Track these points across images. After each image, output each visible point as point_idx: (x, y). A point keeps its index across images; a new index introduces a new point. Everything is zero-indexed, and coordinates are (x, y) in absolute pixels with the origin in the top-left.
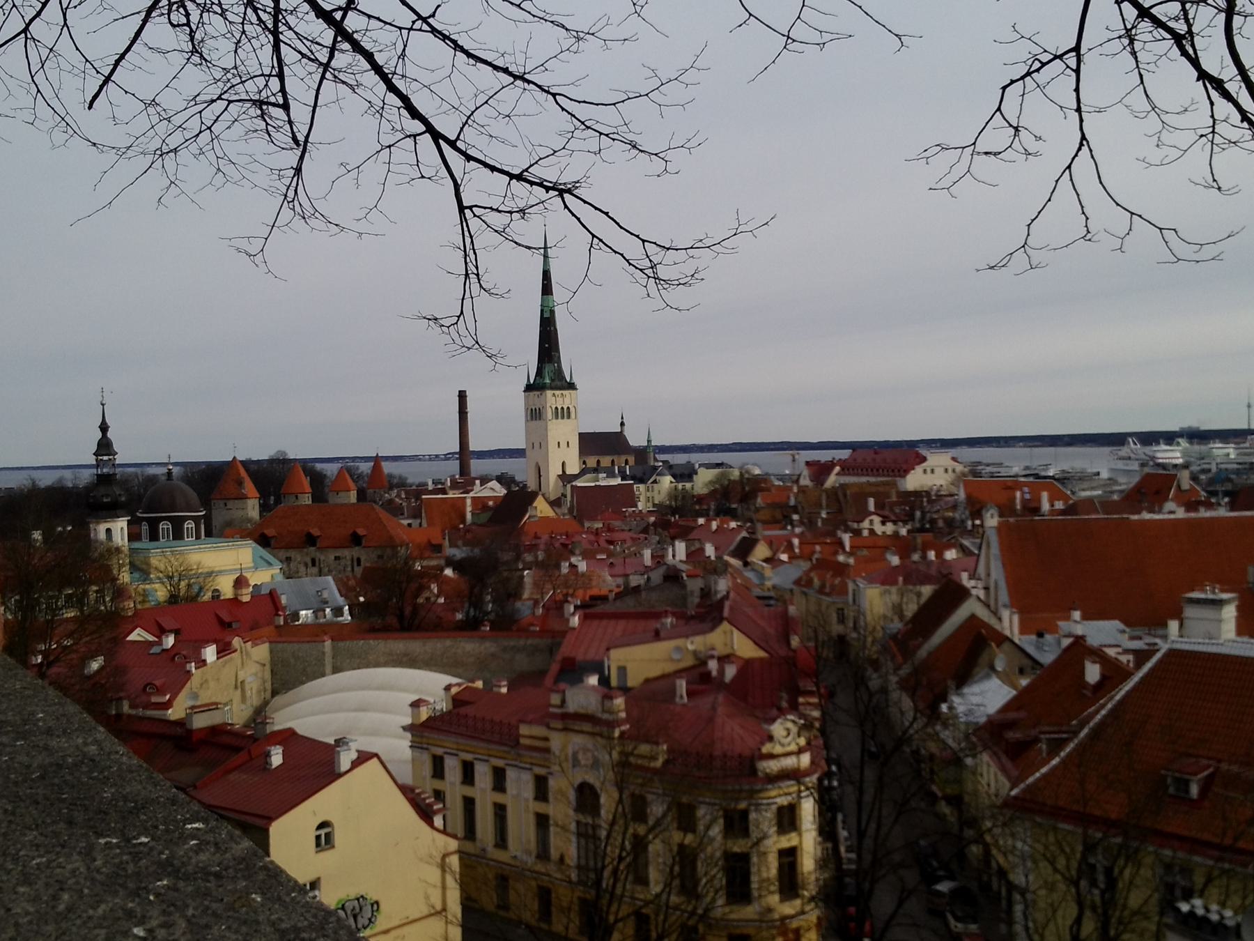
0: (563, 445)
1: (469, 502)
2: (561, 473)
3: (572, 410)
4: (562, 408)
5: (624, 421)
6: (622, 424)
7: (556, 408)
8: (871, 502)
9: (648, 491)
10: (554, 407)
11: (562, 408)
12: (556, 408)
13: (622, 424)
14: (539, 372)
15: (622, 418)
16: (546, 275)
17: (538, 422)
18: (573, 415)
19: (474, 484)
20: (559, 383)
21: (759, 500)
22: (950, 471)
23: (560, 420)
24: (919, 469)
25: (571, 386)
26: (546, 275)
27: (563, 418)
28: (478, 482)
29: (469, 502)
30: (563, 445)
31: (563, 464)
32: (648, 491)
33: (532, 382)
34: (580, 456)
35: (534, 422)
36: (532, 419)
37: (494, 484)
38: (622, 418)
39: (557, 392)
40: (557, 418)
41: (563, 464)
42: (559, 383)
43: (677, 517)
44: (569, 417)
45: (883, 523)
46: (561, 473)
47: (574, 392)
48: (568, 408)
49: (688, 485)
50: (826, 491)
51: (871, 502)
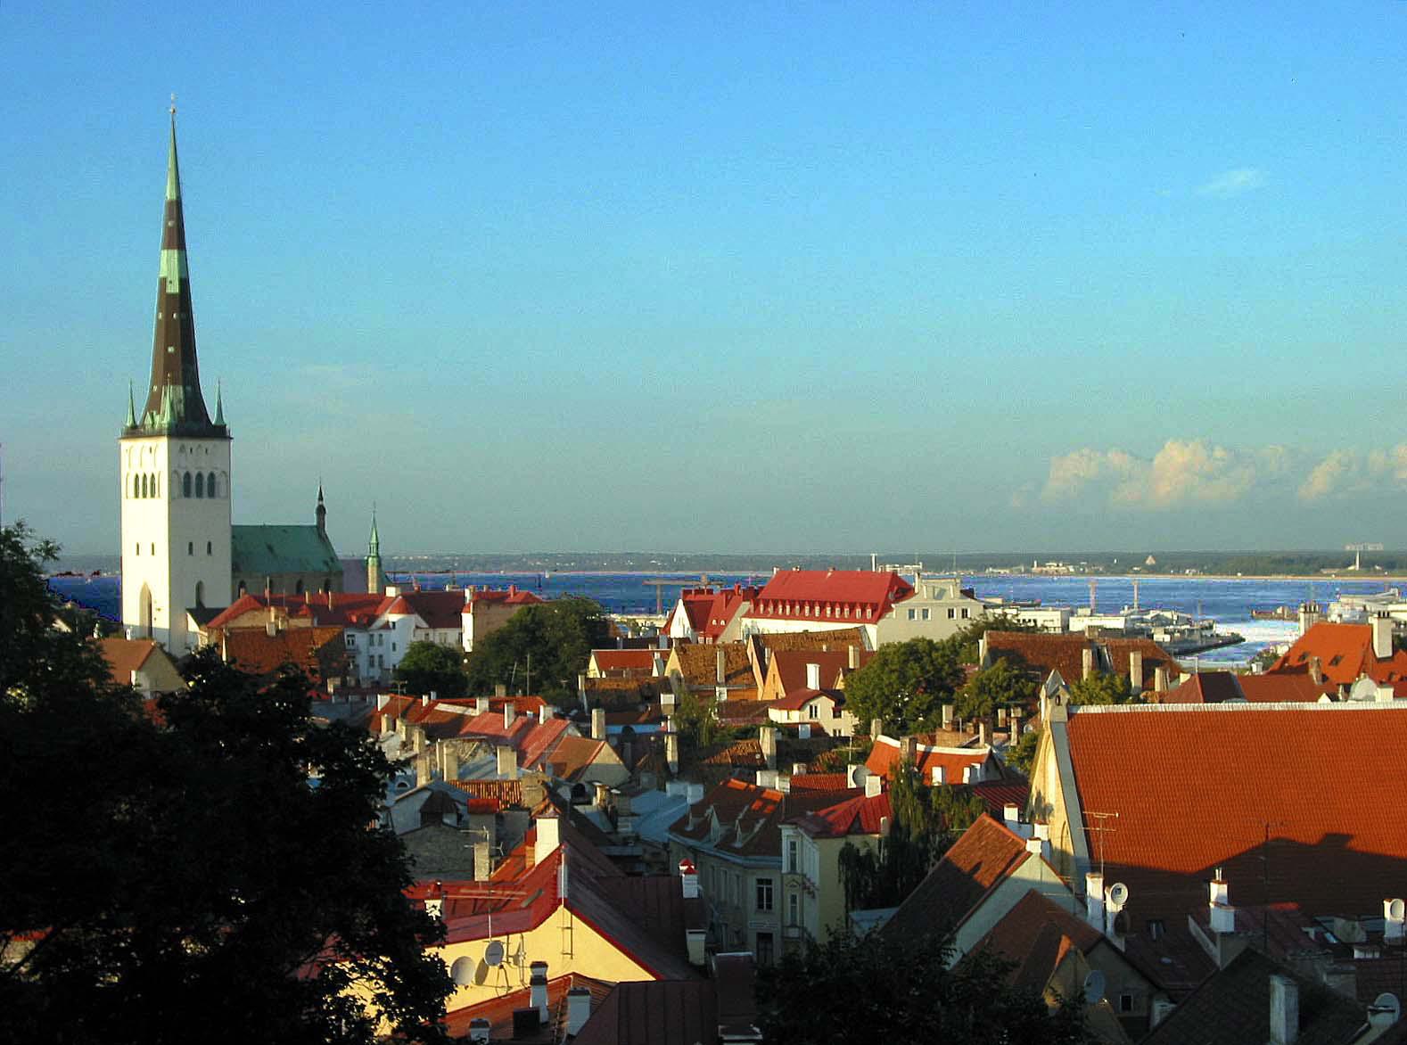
0: (200, 548)
2: (194, 606)
3: (219, 479)
4: (200, 476)
5: (324, 503)
6: (321, 511)
7: (188, 475)
8: (813, 672)
9: (372, 643)
10: (182, 474)
11: (200, 476)
12: (188, 475)
13: (321, 511)
14: (154, 404)
15: (321, 498)
16: (176, 209)
18: (221, 489)
20: (196, 427)
21: (593, 664)
22: (957, 613)
23: (194, 500)
24: (899, 610)
25: (220, 433)
26: (176, 209)
27: (199, 495)
30: (200, 548)
31: (199, 587)
32: (372, 643)
34: (234, 577)
36: (137, 496)
38: (321, 498)
39: (190, 443)
40: (187, 493)
41: (199, 587)
42: (196, 427)
43: (433, 695)
44: (212, 494)
45: (837, 713)
46: (194, 606)
47: (225, 443)
48: (212, 476)
49: (450, 636)
50: (726, 648)
51: (813, 672)
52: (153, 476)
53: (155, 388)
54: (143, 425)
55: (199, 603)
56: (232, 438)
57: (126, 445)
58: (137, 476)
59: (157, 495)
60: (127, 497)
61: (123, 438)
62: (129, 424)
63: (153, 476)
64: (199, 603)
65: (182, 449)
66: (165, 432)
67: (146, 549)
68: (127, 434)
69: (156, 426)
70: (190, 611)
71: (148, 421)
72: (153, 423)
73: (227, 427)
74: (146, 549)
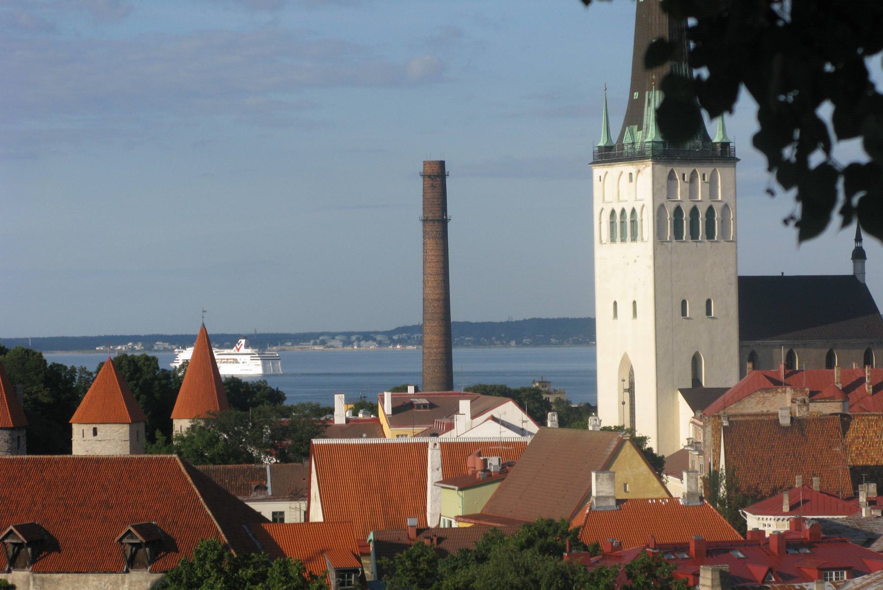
0: (695, 309)
1: (434, 458)
2: (690, 386)
4: (694, 212)
17: (629, 244)
19: (456, 411)
28: (465, 405)
29: (434, 458)
30: (695, 309)
31: (696, 361)
33: (614, 140)
34: (741, 347)
35: (618, 244)
36: (613, 240)
37: (510, 411)
41: (696, 361)
52: (633, 211)
53: (636, 95)
54: (621, 146)
55: (696, 381)
56: (738, 160)
57: (598, 171)
58: (613, 212)
59: (639, 237)
60: (601, 242)
61: (595, 163)
62: (602, 143)
63: (633, 211)
64: (696, 381)
65: (671, 177)
66: (649, 153)
67: (625, 310)
68: (601, 157)
69: (637, 146)
70: (685, 393)
71: (627, 139)
72: (633, 143)
73: (731, 145)
74: (625, 310)
